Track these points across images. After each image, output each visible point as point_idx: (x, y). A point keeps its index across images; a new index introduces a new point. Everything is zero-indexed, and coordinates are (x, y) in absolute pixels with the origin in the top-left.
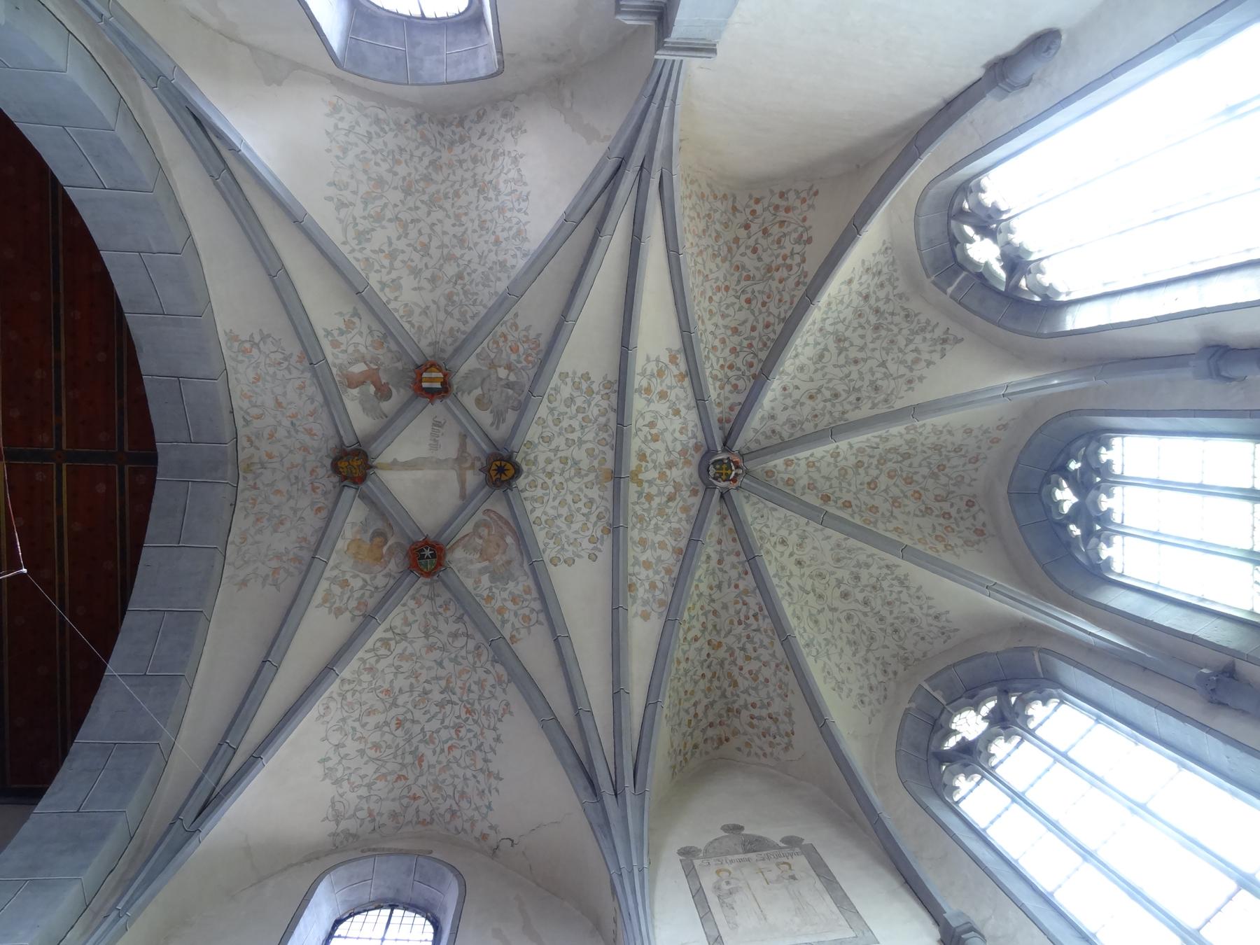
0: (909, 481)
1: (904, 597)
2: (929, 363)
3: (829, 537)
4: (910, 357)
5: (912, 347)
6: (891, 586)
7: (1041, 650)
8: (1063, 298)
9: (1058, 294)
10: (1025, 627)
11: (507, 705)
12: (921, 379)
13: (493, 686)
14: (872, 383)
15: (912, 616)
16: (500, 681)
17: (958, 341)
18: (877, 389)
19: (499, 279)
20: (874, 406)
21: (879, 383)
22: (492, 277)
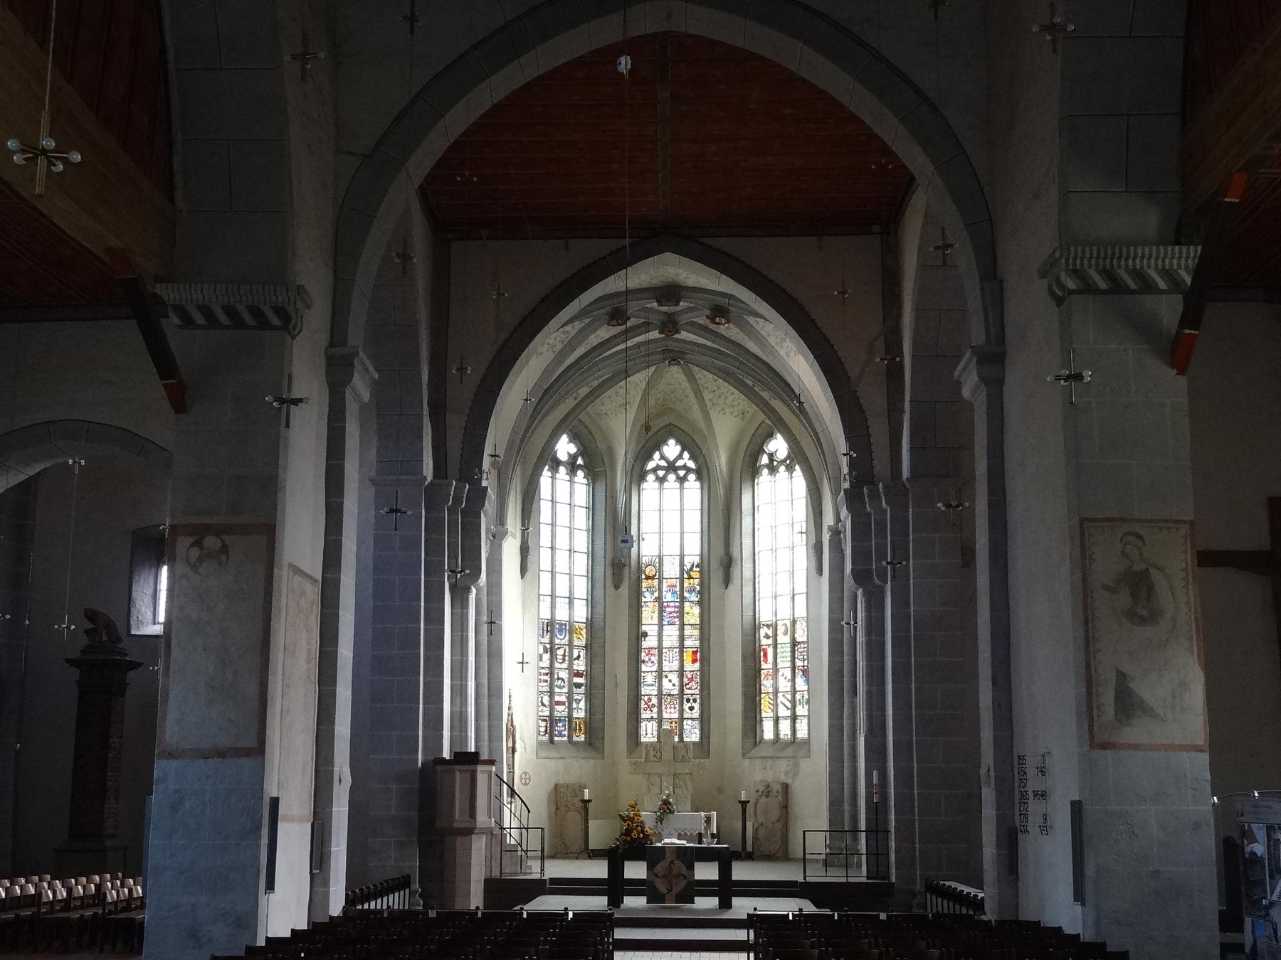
0: (672, 392)
1: (614, 404)
2: (732, 413)
3: (641, 381)
4: (736, 403)
5: (740, 401)
6: (619, 400)
7: (605, 471)
8: (756, 481)
9: (758, 478)
10: (611, 451)
11: (541, 354)
12: (724, 414)
13: (548, 344)
14: (723, 393)
15: (605, 404)
16: (554, 346)
17: (743, 419)
18: (719, 397)
19: (776, 338)
20: (710, 400)
21: (722, 397)
22: (778, 332)
